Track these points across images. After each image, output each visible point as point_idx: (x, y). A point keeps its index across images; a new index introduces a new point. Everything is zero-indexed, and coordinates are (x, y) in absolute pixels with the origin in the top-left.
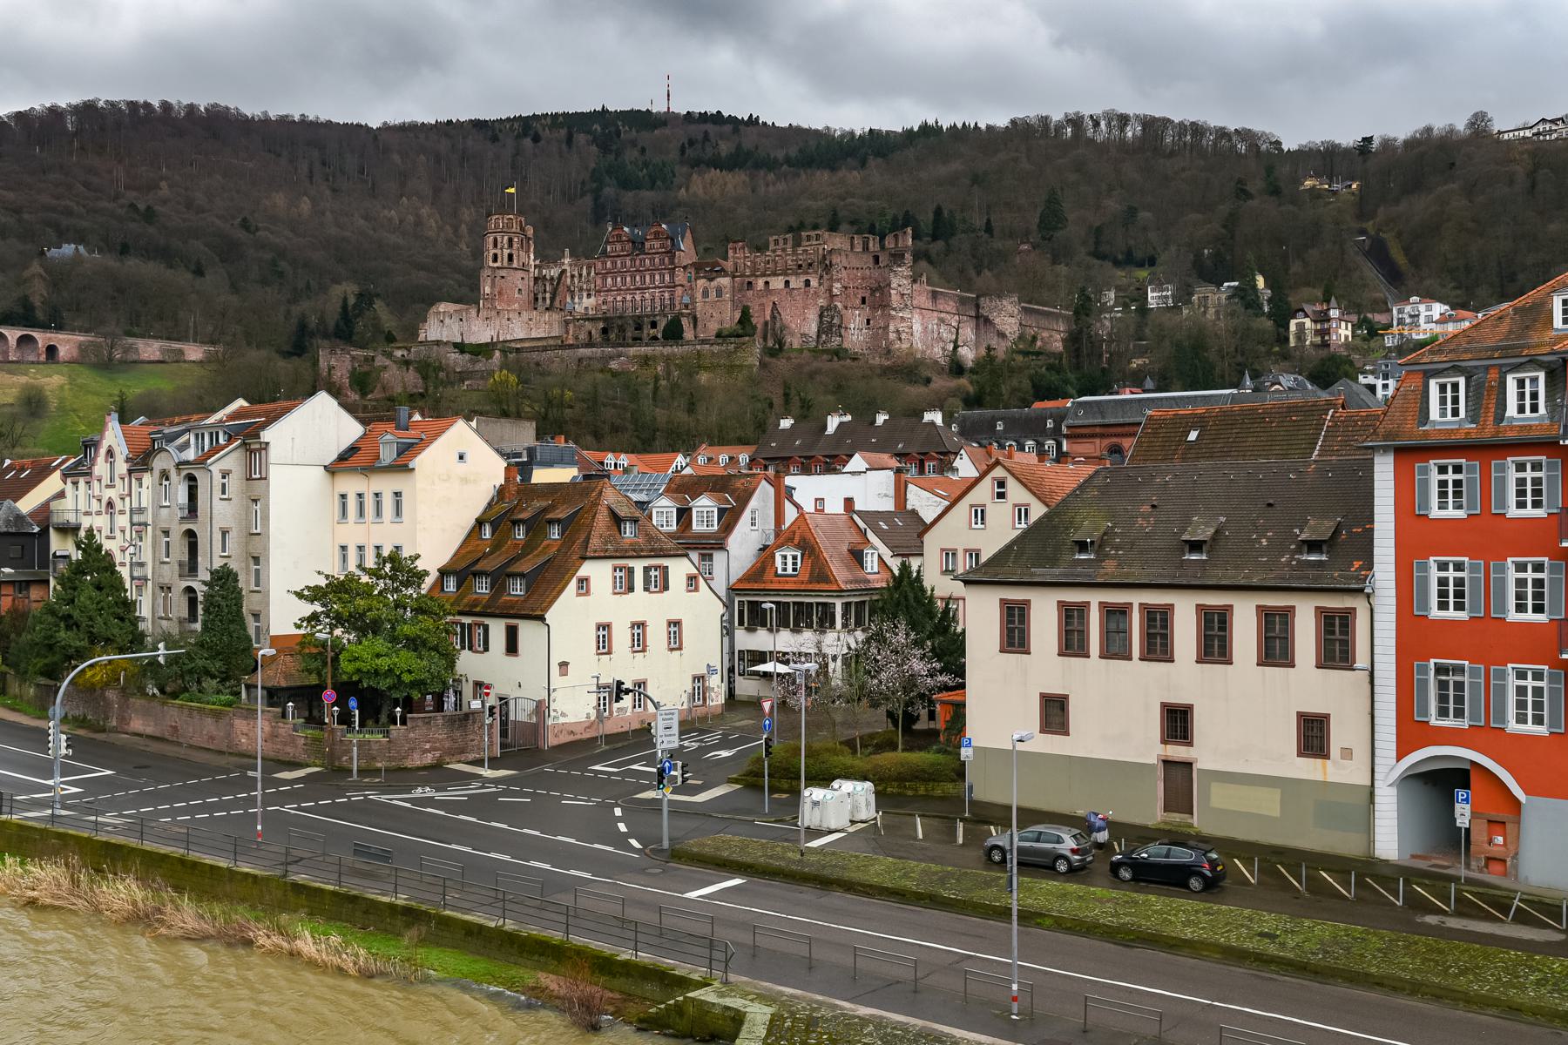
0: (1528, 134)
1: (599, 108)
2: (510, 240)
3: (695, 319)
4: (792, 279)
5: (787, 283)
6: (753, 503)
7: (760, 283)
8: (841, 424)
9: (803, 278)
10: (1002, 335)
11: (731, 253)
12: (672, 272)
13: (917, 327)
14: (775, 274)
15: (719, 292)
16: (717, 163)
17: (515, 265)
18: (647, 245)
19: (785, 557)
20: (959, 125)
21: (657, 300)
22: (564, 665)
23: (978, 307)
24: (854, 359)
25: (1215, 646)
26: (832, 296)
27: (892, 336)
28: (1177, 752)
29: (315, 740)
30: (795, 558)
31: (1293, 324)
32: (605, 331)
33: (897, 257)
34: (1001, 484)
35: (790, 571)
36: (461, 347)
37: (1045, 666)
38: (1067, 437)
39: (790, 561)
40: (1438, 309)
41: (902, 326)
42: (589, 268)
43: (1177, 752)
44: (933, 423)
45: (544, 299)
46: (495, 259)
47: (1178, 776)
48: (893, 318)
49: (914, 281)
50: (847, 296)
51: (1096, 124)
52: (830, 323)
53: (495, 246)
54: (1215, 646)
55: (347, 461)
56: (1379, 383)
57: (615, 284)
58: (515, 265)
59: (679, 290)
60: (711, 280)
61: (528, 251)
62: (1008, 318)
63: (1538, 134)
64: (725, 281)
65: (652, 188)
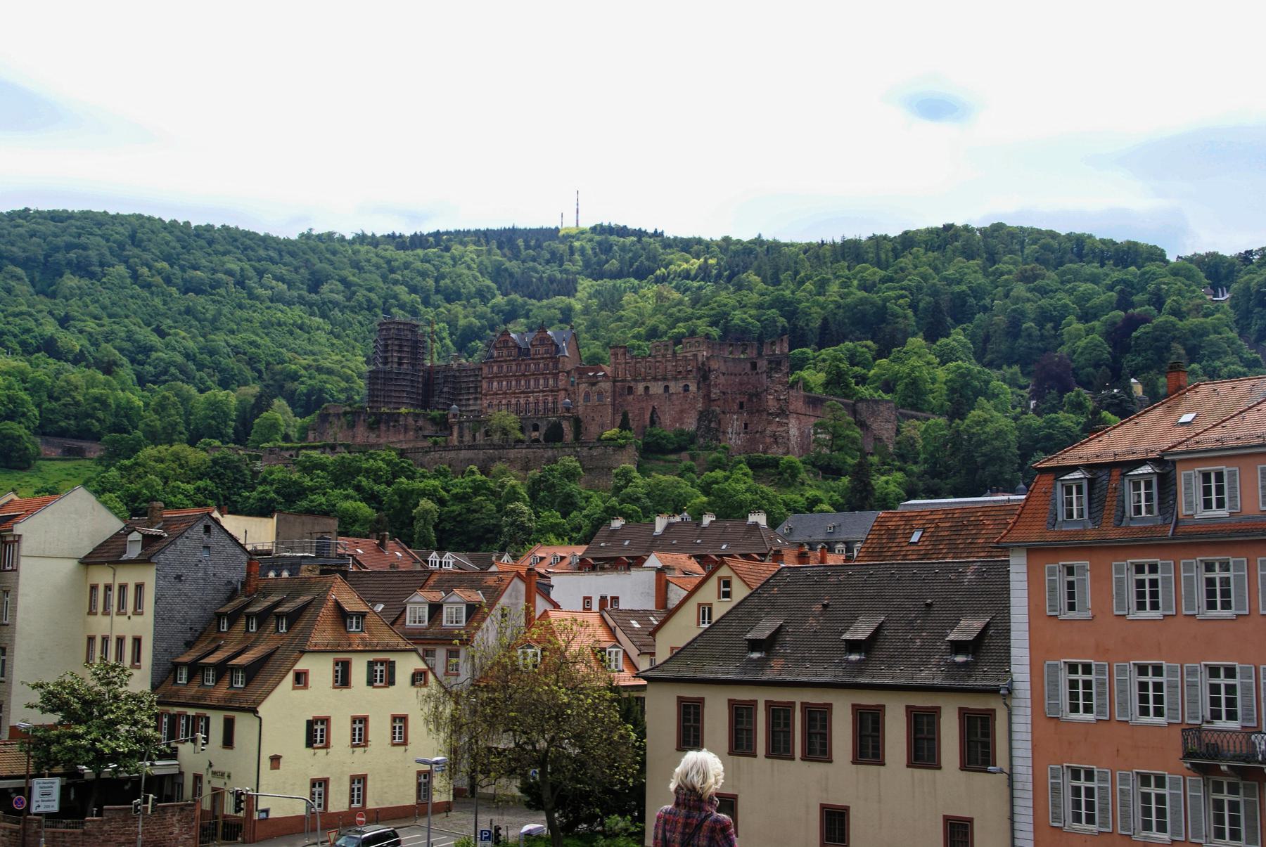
5: (667, 388)
6: (504, 601)
7: (640, 388)
12: (555, 376)
13: (794, 432)
14: (655, 379)
22: (275, 760)
25: (868, 748)
34: (727, 583)
44: (756, 525)
48: (770, 423)
50: (726, 401)
54: (868, 748)
55: (106, 554)
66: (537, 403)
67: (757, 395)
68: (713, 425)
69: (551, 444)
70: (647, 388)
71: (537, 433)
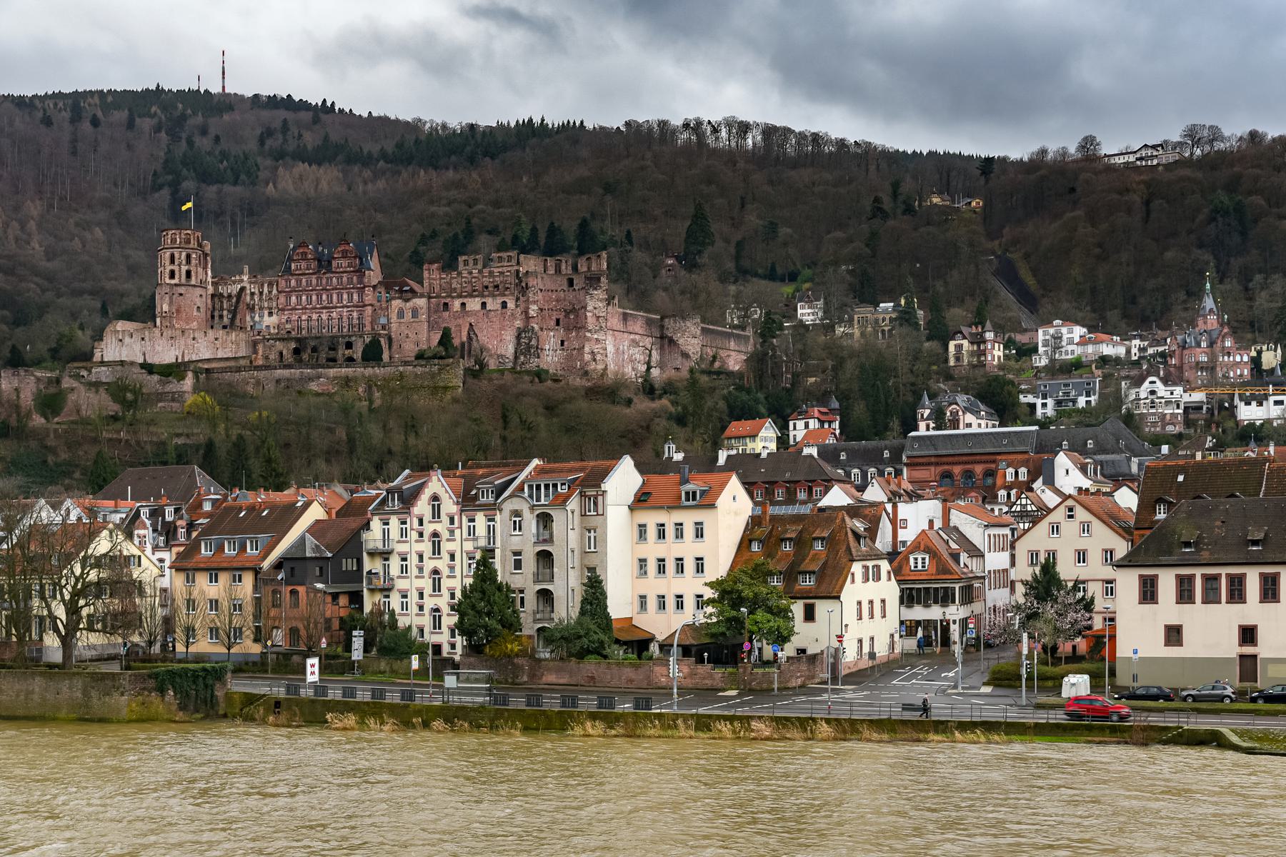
0: (1132, 158)
1: (153, 87)
2: (188, 256)
3: (390, 340)
4: (489, 301)
5: (484, 304)
7: (456, 304)
8: (729, 457)
9: (500, 300)
10: (686, 355)
11: (426, 274)
12: (361, 290)
13: (610, 349)
14: (471, 296)
15: (415, 312)
16: (302, 156)
17: (193, 282)
18: (334, 264)
20: (537, 120)
21: (345, 319)
23: (662, 327)
24: (556, 381)
26: (528, 318)
27: (587, 357)
28: (1248, 650)
29: (731, 674)
31: (952, 344)
32: (297, 351)
33: (593, 281)
34: (1071, 510)
35: (920, 567)
36: (148, 368)
37: (1168, 608)
38: (906, 465)
39: (920, 561)
40: (1079, 331)
41: (597, 348)
42: (270, 285)
43: (1248, 650)
44: (811, 456)
45: (221, 317)
46: (172, 275)
47: (1248, 664)
48: (589, 340)
49: (608, 304)
50: (543, 318)
51: (715, 130)
52: (526, 344)
53: (172, 262)
56: (1039, 402)
57: (299, 303)
58: (193, 282)
59: (369, 310)
60: (407, 300)
61: (205, 268)
62: (691, 338)
63: (1141, 159)
64: (421, 302)
65: (235, 183)
66: (341, 319)
68: (533, 342)
70: (463, 304)
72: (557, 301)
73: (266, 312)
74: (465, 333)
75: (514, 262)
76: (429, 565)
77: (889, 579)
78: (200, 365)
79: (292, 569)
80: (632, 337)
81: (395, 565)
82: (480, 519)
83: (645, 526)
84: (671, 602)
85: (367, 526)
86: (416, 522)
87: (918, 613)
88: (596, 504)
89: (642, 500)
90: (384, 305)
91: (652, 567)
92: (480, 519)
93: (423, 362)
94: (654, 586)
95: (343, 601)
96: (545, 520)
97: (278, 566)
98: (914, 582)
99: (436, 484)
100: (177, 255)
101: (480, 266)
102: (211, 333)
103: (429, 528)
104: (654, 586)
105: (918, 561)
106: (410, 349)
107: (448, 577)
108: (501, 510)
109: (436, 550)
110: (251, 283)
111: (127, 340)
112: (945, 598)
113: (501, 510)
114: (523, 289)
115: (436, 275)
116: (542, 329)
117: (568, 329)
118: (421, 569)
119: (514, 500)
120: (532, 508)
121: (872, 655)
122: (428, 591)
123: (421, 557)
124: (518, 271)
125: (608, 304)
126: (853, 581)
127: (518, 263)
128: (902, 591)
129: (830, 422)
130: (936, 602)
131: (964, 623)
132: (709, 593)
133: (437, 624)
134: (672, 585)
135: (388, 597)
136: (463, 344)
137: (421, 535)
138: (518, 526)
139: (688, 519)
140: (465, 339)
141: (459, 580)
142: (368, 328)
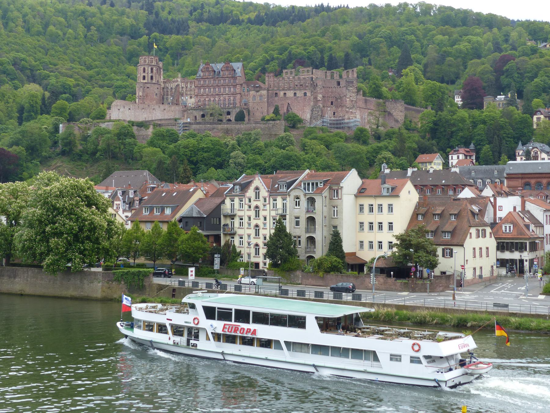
2: (152, 69)
5: (295, 94)
10: (397, 121)
11: (267, 79)
12: (235, 86)
14: (289, 89)
17: (154, 81)
19: (506, 227)
29: (405, 283)
30: (510, 227)
31: (535, 118)
33: (349, 83)
35: (508, 231)
39: (508, 228)
44: (456, 172)
46: (144, 78)
48: (347, 112)
49: (357, 95)
53: (144, 72)
58: (154, 81)
60: (257, 91)
61: (160, 75)
64: (264, 92)
66: (225, 100)
67: (341, 98)
69: (240, 122)
70: (285, 94)
71: (229, 116)
72: (332, 93)
73: (189, 97)
74: (285, 108)
75: (310, 73)
76: (254, 222)
77: (491, 237)
78: (156, 122)
79: (186, 222)
80: (369, 111)
81: (237, 221)
82: (279, 200)
83: (363, 205)
84: (376, 245)
85: (223, 202)
86: (247, 200)
87: (507, 255)
88: (337, 193)
89: (361, 192)
90: (246, 94)
91: (366, 226)
92: (279, 200)
93: (265, 122)
94: (367, 236)
95: (211, 239)
96: (311, 201)
97: (180, 221)
98: (505, 238)
99: (258, 181)
100: (146, 69)
101: (293, 75)
102: (162, 107)
103: (253, 204)
104: (367, 236)
105: (507, 228)
106: (258, 116)
107: (263, 229)
108: (289, 196)
109: (257, 215)
110: (182, 82)
111: (122, 109)
112: (521, 247)
113: (289, 196)
114: (314, 86)
115: (272, 79)
116: (324, 107)
117: (337, 107)
118: (249, 224)
119: (296, 190)
120: (305, 195)
121: (481, 276)
122: (253, 235)
123: (250, 218)
124: (312, 78)
125: (357, 95)
126: (471, 237)
127: (312, 74)
128: (498, 243)
129: (470, 156)
130: (516, 250)
131: (531, 261)
132: (395, 241)
133: (257, 252)
134: (376, 236)
135: (233, 238)
136: (284, 114)
137: (250, 207)
138: (298, 204)
139: (385, 202)
140: (285, 111)
141: (268, 231)
142: (238, 105)
